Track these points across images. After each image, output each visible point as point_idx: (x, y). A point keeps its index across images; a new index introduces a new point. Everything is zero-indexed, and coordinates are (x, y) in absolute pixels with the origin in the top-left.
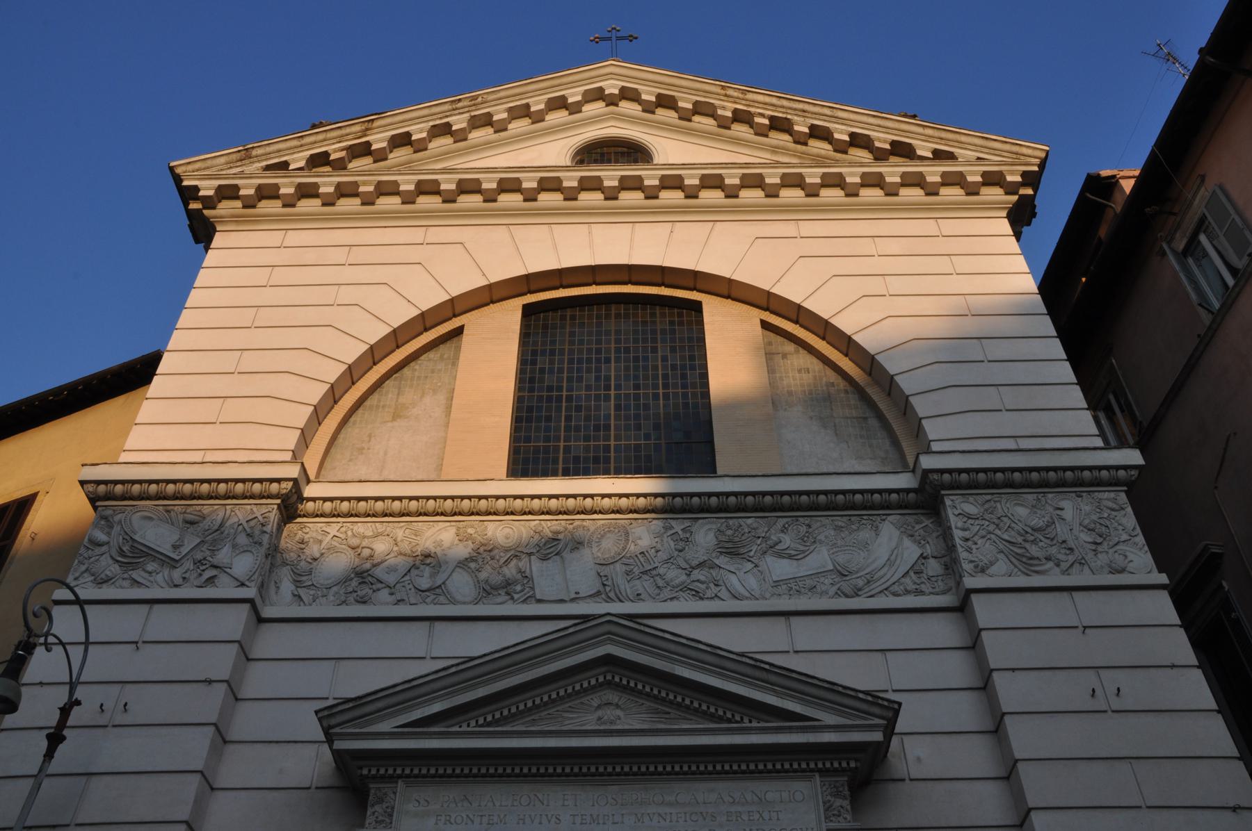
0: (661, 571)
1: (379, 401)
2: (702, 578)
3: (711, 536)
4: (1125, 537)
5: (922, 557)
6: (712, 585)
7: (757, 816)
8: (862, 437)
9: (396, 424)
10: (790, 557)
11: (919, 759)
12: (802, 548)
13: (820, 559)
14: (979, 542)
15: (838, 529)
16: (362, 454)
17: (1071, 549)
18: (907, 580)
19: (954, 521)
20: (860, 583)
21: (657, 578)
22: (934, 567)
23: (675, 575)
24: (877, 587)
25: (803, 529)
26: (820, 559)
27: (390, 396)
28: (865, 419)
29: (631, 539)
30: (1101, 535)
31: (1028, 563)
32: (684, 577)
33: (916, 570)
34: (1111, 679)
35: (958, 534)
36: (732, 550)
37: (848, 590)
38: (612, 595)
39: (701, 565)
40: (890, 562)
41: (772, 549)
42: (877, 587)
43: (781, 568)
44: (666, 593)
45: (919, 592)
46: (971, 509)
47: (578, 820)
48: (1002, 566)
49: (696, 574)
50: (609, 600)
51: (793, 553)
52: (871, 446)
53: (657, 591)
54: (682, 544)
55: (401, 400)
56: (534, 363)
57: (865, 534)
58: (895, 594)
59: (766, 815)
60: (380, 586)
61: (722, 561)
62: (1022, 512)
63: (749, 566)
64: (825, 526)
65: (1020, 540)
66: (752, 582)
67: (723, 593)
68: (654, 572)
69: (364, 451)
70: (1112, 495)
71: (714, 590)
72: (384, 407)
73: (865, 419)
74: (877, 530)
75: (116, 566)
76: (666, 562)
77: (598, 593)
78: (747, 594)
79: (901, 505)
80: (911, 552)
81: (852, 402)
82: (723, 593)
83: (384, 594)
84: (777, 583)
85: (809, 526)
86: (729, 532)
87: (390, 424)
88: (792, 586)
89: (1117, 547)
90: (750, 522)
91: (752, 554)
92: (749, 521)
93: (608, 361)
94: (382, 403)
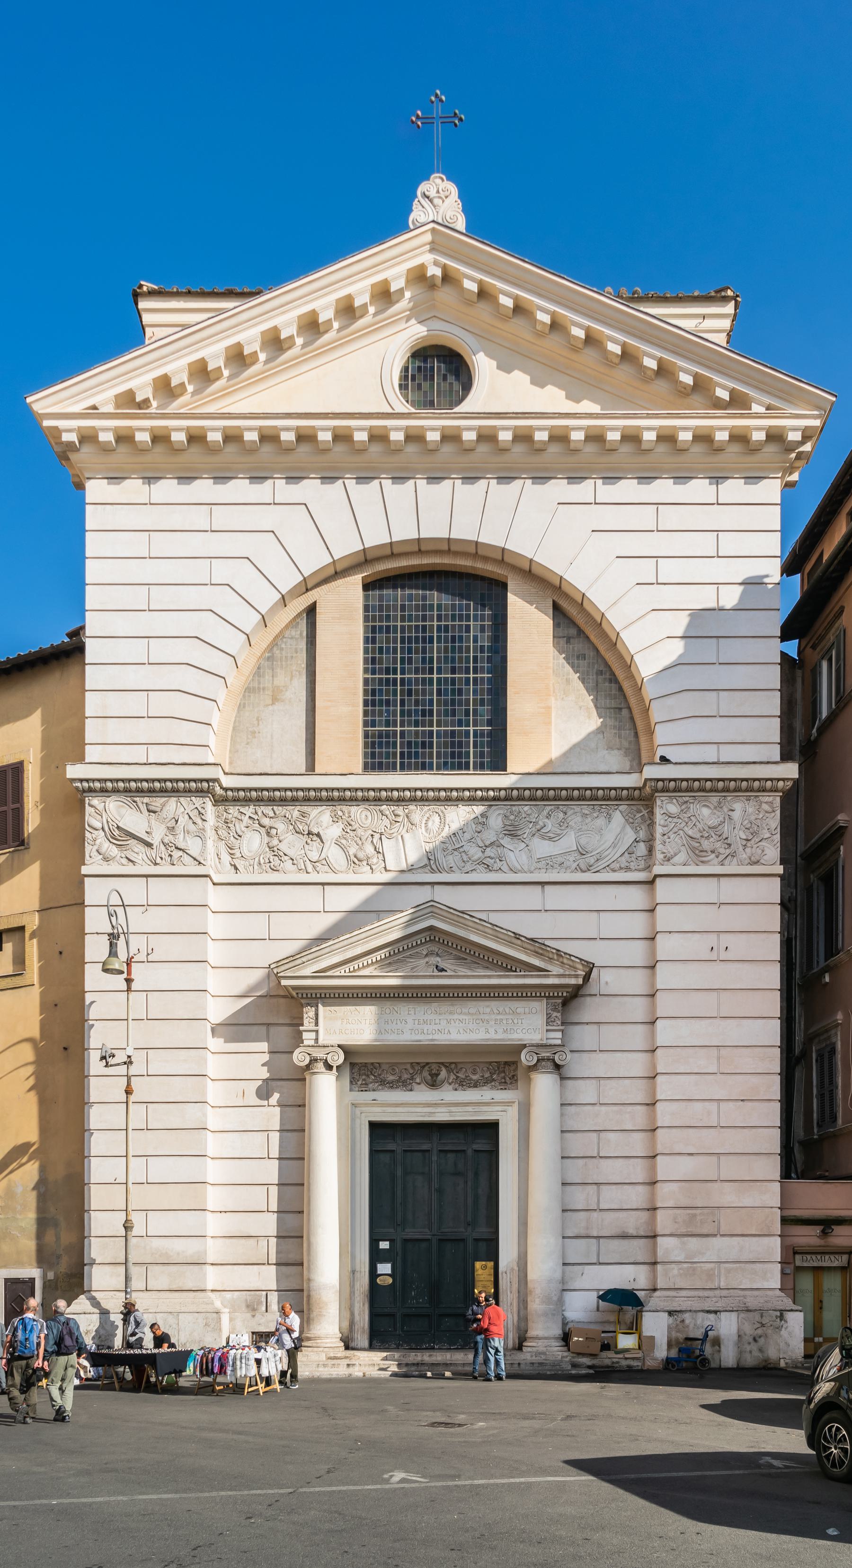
0: (465, 848)
1: (259, 683)
2: (492, 855)
3: (500, 818)
4: (767, 835)
5: (636, 841)
6: (498, 860)
7: (511, 1021)
8: (615, 727)
9: (276, 707)
10: (550, 839)
11: (607, 983)
12: (559, 832)
13: (569, 842)
14: (672, 837)
15: (585, 816)
16: (255, 737)
17: (730, 845)
18: (623, 859)
19: (659, 818)
20: (592, 861)
21: (463, 854)
22: (642, 849)
23: (475, 852)
24: (602, 864)
25: (561, 815)
26: (569, 842)
27: (267, 677)
28: (620, 709)
29: (447, 822)
30: (753, 832)
31: (698, 854)
32: (480, 854)
33: (630, 852)
34: (726, 939)
35: (659, 830)
36: (512, 832)
37: (583, 867)
38: (434, 867)
39: (492, 844)
40: (614, 845)
41: (539, 832)
42: (602, 864)
43: (542, 848)
44: (469, 867)
45: (628, 869)
46: (673, 808)
47: (416, 1022)
48: (682, 857)
49: (489, 852)
50: (433, 871)
51: (552, 835)
52: (620, 737)
53: (463, 864)
54: (480, 828)
55: (277, 682)
56: (374, 641)
57: (601, 822)
58: (614, 871)
59: (515, 1021)
60: (286, 858)
61: (506, 841)
62: (706, 812)
63: (523, 845)
64: (576, 813)
65: (698, 836)
66: (524, 858)
67: (505, 868)
68: (461, 850)
69: (257, 735)
70: (771, 799)
71: (499, 864)
72: (264, 689)
73: (620, 709)
74: (609, 817)
75: (114, 847)
76: (470, 841)
77: (425, 866)
78: (520, 868)
79: (630, 798)
80: (630, 836)
81: (613, 692)
82: (505, 868)
83: (288, 864)
84: (539, 860)
85: (565, 813)
86: (512, 817)
87: (270, 708)
88: (549, 863)
89: (760, 843)
90: (526, 808)
91: (525, 836)
92: (526, 808)
93: (431, 641)
94: (261, 686)
